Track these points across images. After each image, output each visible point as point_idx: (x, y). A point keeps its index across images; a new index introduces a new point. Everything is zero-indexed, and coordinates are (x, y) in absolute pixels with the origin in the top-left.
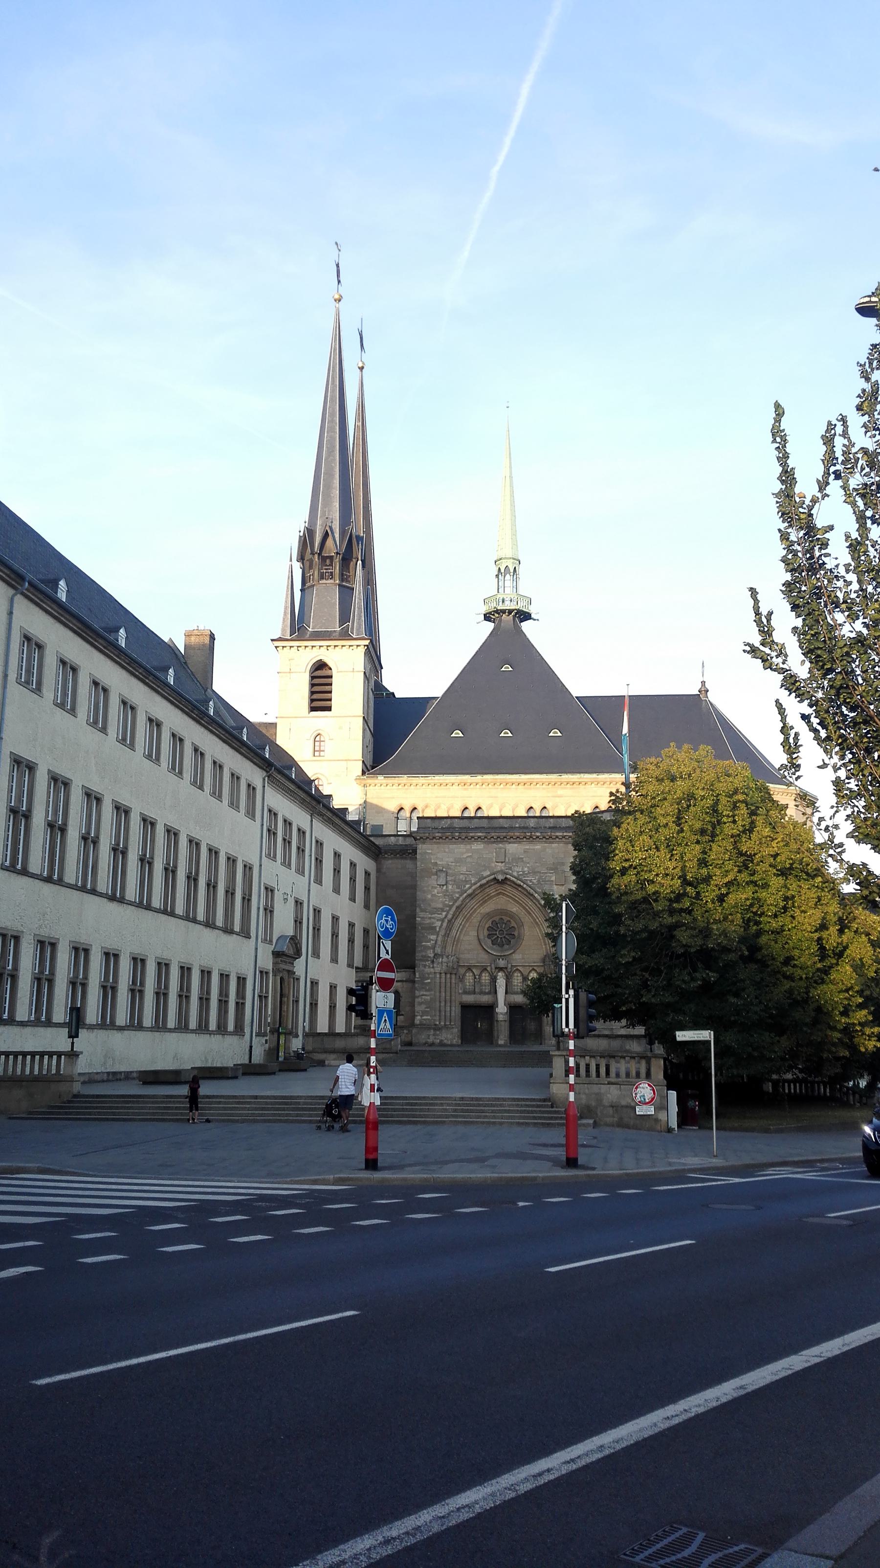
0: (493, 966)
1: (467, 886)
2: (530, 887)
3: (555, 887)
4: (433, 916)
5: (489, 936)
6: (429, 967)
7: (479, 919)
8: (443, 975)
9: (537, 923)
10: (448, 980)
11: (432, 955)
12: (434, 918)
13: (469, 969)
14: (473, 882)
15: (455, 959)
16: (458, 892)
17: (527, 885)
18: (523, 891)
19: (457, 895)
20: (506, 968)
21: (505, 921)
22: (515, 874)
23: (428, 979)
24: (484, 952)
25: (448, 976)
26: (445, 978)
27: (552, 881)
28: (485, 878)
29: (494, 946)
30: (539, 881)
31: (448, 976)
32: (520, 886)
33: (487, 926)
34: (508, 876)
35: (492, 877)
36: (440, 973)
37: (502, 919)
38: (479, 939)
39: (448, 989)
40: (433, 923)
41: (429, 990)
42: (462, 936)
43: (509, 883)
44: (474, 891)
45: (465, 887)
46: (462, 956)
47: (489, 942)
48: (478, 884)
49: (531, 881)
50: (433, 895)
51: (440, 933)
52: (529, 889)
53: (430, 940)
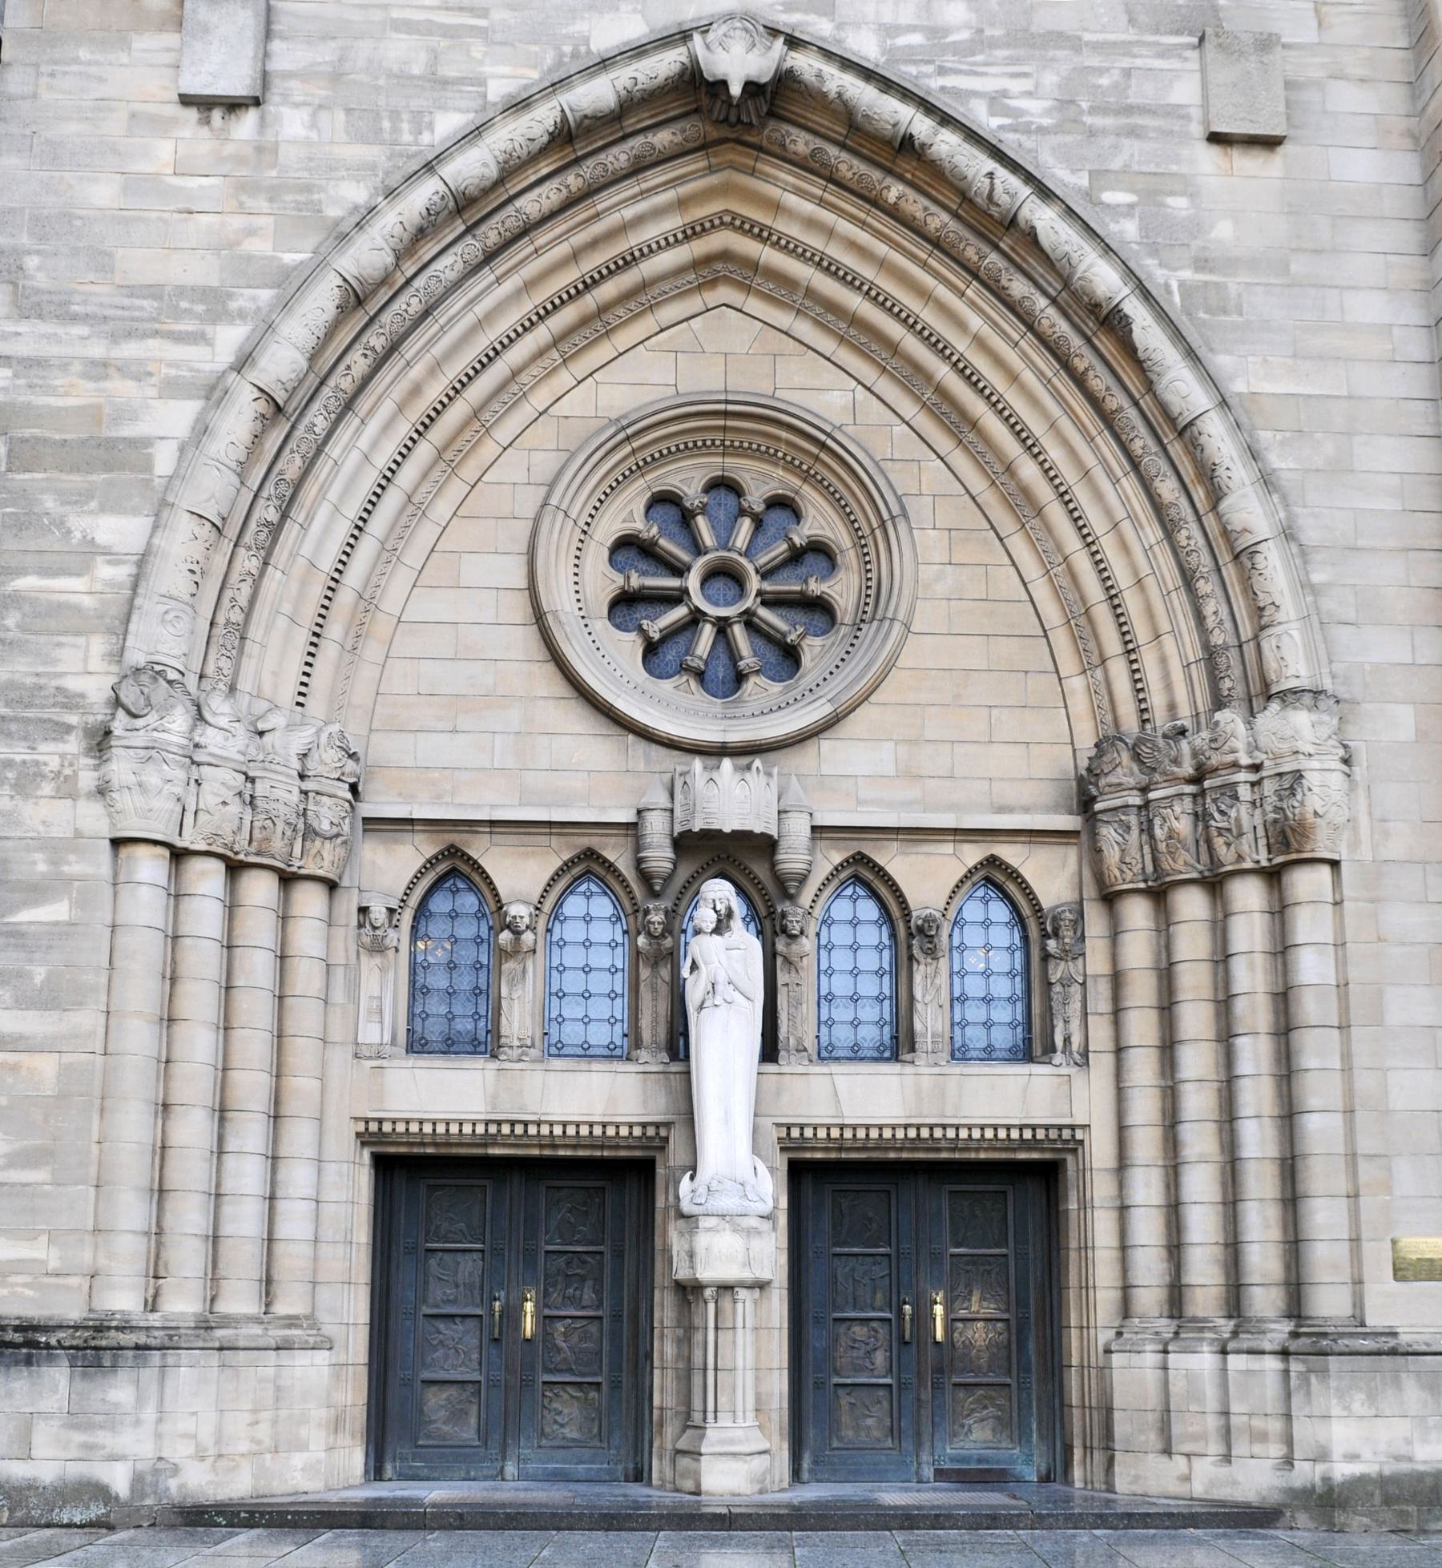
0: (657, 829)
1: (449, 123)
2: (997, 154)
3: (1212, 155)
4: (130, 350)
5: (625, 604)
6: (67, 789)
7: (546, 464)
8: (207, 877)
9: (1022, 503)
10: (258, 927)
11: (95, 687)
12: (137, 372)
13: (453, 852)
14: (498, 90)
15: (332, 756)
16: (373, 167)
17: (972, 136)
18: (915, 205)
19: (357, 193)
20: (766, 845)
21: (755, 499)
22: (866, 47)
23: (38, 892)
24: (575, 719)
25: (260, 889)
26: (232, 907)
27: (1176, 112)
28: (604, 64)
29: (667, 685)
30: (1065, 103)
31: (260, 889)
32: (907, 146)
33: (610, 528)
34: (805, 64)
35: (664, 65)
36: (178, 855)
37: (723, 485)
38: (539, 617)
39: (254, 1008)
40: (130, 414)
41: (49, 1000)
42: (398, 585)
43: (801, 142)
44: (510, 169)
45: (421, 123)
46: (385, 748)
47: (630, 645)
48: (542, 120)
49: (996, 101)
50: (133, 184)
51: (188, 498)
52: (975, 166)
53: (91, 551)
